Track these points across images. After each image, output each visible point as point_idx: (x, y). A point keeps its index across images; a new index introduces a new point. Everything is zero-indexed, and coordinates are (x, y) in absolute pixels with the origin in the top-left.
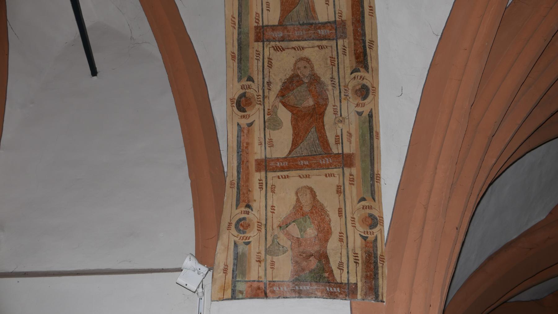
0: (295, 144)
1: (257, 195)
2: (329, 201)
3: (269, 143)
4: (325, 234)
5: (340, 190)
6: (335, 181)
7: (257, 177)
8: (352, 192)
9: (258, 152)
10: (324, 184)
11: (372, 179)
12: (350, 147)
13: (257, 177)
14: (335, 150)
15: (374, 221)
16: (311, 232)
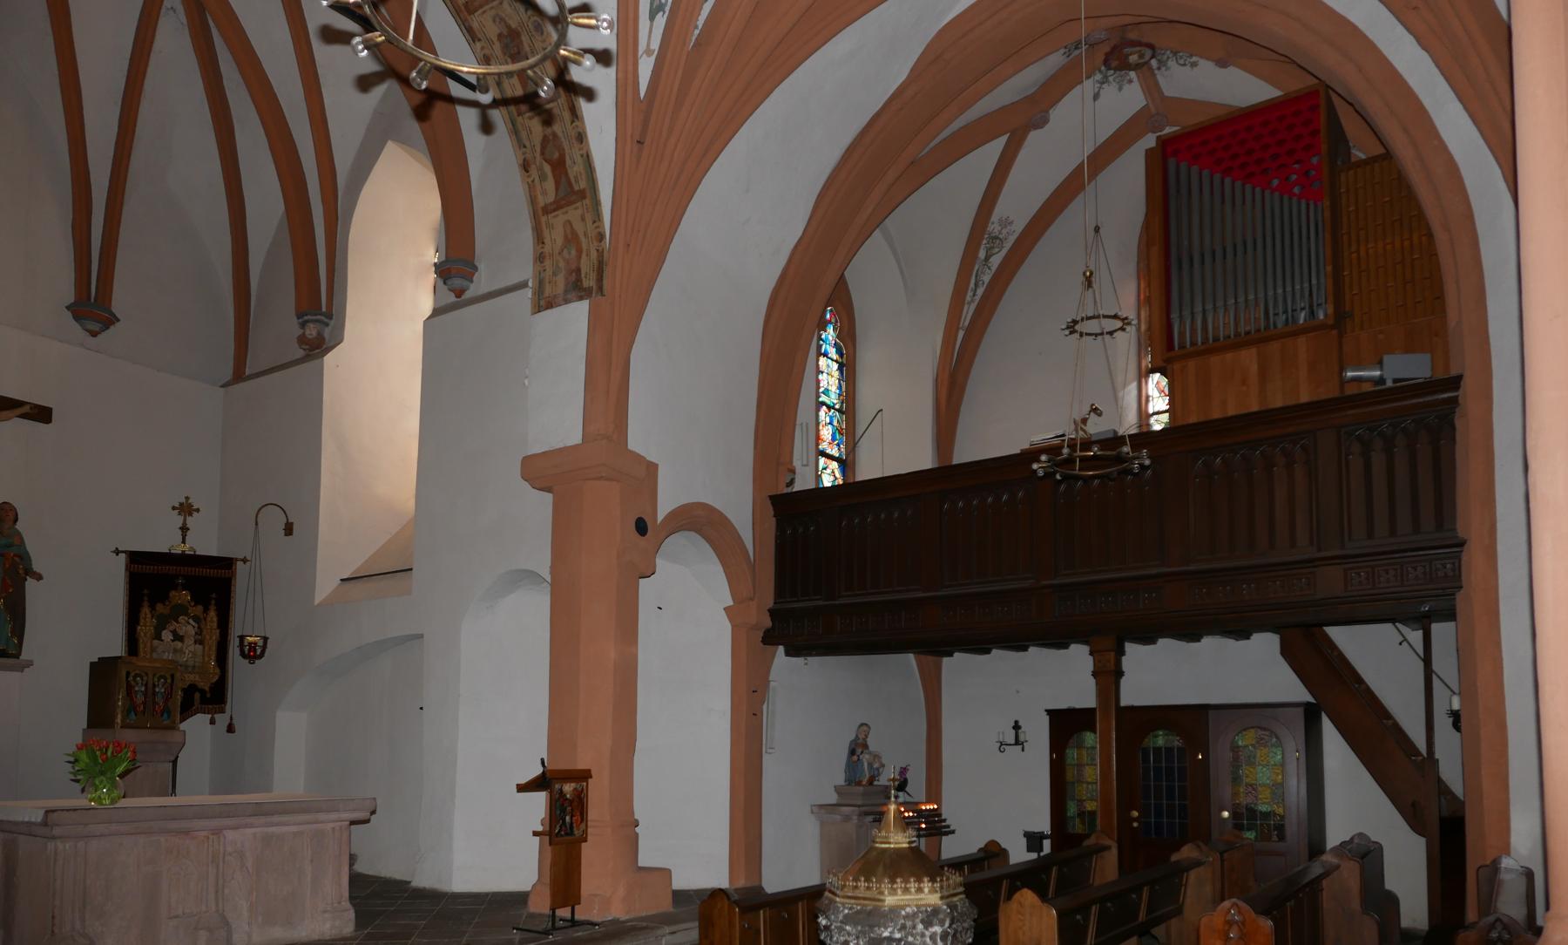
0: (557, 189)
1: (546, 233)
2: (579, 227)
3: (544, 193)
4: (579, 251)
5: (583, 219)
6: (579, 212)
7: (544, 219)
8: (589, 218)
9: (541, 201)
10: (573, 214)
11: (597, 203)
12: (583, 184)
13: (544, 219)
14: (576, 188)
15: (601, 237)
16: (574, 252)
